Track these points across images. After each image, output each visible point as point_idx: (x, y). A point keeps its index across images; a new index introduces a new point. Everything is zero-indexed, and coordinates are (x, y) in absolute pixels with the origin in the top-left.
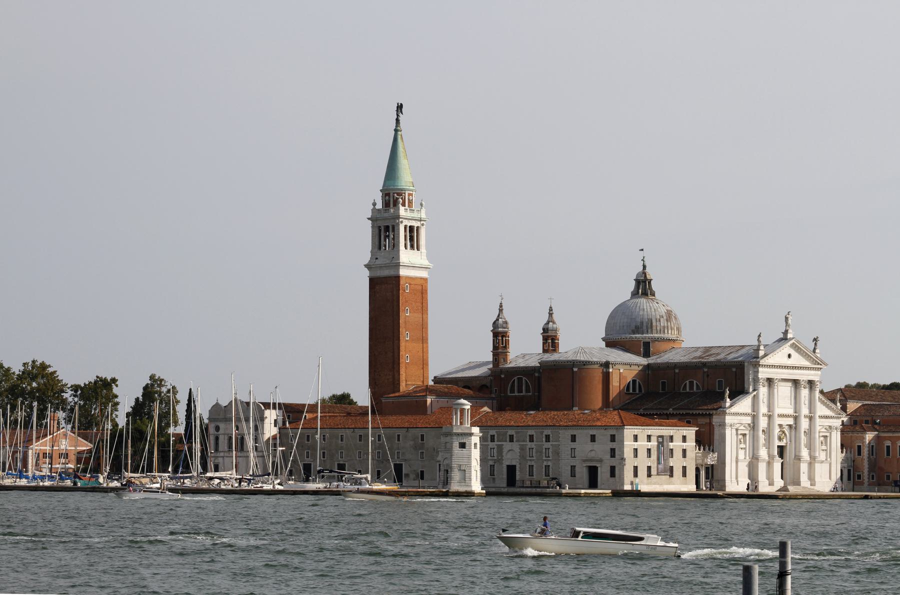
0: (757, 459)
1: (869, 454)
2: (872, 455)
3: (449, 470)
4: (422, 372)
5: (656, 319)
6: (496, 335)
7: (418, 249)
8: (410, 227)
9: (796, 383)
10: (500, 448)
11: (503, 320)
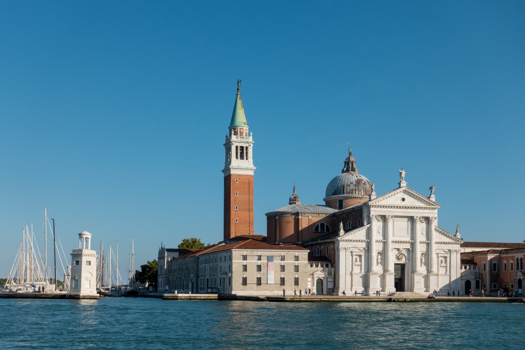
1: (491, 270)
2: (495, 269)
7: (247, 159)
9: (412, 219)
11: (294, 196)
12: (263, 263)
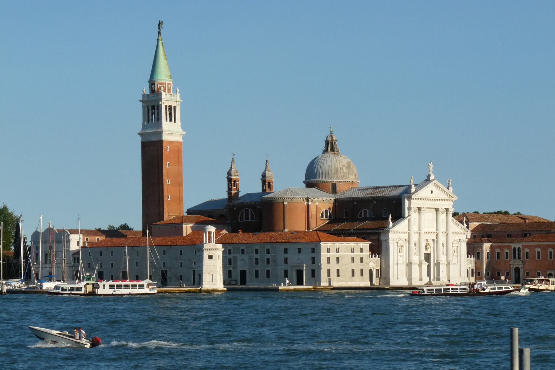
0: (411, 263)
3: (201, 275)
4: (179, 206)
5: (341, 168)
6: (230, 180)
7: (175, 121)
8: (169, 106)
9: (437, 210)
10: (235, 258)
11: (235, 170)
12: (341, 255)
